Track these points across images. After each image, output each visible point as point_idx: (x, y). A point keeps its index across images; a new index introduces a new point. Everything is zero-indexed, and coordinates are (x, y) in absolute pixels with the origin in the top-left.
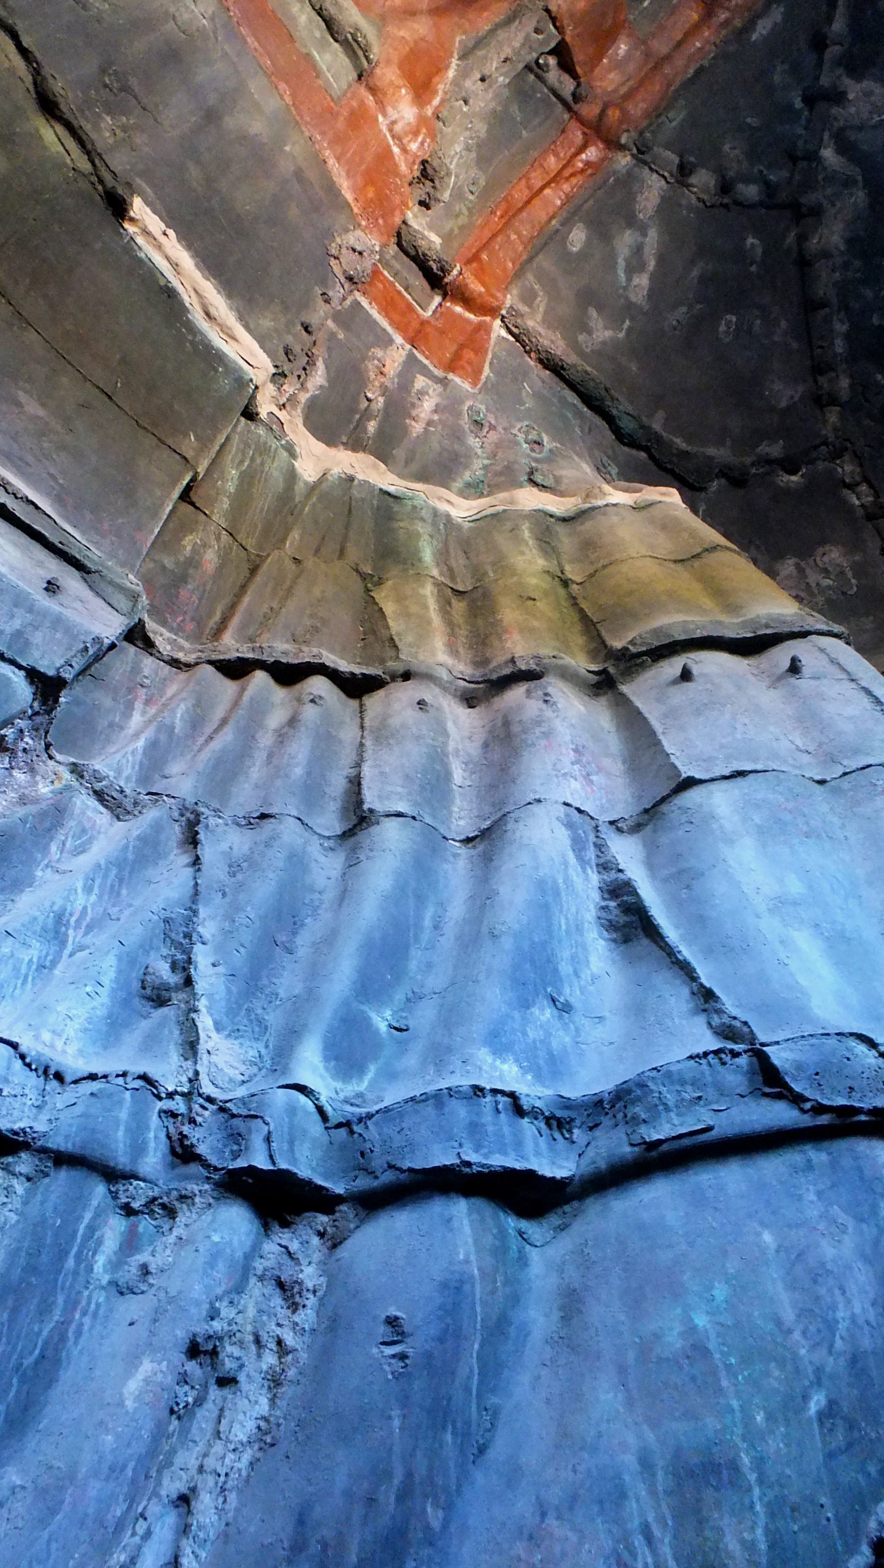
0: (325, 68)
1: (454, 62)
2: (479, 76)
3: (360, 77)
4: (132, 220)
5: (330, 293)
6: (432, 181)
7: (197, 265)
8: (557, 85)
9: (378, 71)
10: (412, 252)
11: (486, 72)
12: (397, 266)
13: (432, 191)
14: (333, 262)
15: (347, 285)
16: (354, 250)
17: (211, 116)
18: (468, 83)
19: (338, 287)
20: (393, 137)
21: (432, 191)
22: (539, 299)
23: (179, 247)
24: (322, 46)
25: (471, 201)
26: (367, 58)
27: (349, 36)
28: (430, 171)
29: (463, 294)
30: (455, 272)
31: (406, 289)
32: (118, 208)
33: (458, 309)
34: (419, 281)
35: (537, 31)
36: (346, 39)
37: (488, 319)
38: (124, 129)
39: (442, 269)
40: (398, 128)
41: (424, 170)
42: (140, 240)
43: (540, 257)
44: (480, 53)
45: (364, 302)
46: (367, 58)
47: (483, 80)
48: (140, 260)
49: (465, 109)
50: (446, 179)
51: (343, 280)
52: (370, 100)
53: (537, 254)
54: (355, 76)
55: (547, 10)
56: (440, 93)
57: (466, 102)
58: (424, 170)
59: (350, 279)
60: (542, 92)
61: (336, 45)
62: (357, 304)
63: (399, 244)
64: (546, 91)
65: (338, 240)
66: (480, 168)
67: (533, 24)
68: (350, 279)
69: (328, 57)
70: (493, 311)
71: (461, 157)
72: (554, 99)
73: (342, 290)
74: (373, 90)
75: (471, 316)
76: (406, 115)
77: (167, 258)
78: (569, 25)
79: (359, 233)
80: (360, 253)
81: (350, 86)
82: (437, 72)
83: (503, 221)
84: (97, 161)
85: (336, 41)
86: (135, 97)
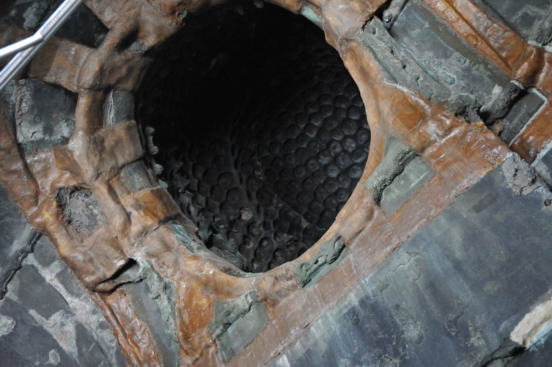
0: (418, 180)
1: (398, 86)
2: (403, 70)
3: (417, 155)
4: (524, 343)
5: (544, 198)
6: (465, 107)
7: (543, 301)
8: (398, 8)
9: (414, 147)
10: (507, 110)
11: (400, 66)
12: (516, 121)
13: (471, 107)
14: (525, 193)
15: (538, 184)
16: (515, 175)
17: (458, 266)
18: (409, 78)
19: (538, 190)
20: (446, 135)
21: (471, 107)
22: (529, 12)
23: (534, 312)
24: (407, 180)
25: (470, 62)
26: (408, 152)
27: (400, 163)
28: (461, 110)
29: (531, 77)
30: (517, 84)
31: (530, 115)
32: (519, 351)
33: (542, 76)
34: (524, 106)
35: (374, 33)
36: (402, 165)
37: (546, 55)
38: (475, 330)
39: (515, 91)
40: (440, 133)
41: (460, 114)
42: (535, 339)
43: (500, 11)
44: (392, 70)
45: (543, 153)
46: (408, 152)
47: (404, 67)
48: (547, 342)
49: (421, 79)
50: (464, 98)
51: (534, 186)
52: (429, 151)
53: (499, 14)
54: (417, 158)
55: (363, 27)
56: (417, 99)
57: (418, 78)
58: (460, 114)
59: (534, 182)
60: (402, 15)
61: (405, 170)
62: (545, 159)
63: (502, 118)
64: (402, 13)
65: (511, 185)
66: (450, 56)
67: (371, 35)
68: (534, 182)
69: (412, 177)
70: (541, 52)
71: (445, 69)
72: (406, 7)
73: (541, 188)
74: (423, 150)
75: (545, 69)
76: (434, 128)
77: (542, 323)
78: (368, 12)
79: (504, 167)
80: (516, 170)
81: (423, 163)
82: (406, 99)
83: (479, 39)
84: (496, 356)
85: (403, 170)
86: (458, 317)
